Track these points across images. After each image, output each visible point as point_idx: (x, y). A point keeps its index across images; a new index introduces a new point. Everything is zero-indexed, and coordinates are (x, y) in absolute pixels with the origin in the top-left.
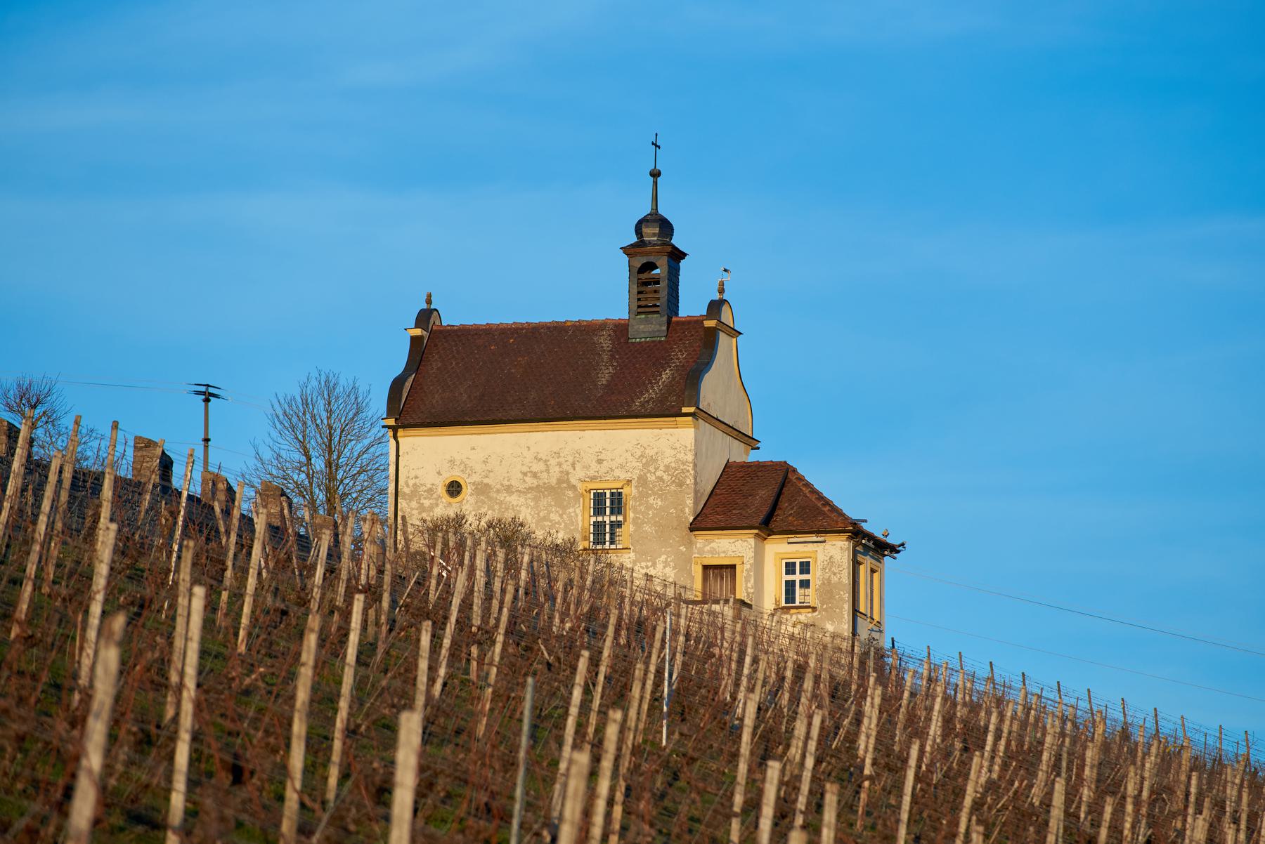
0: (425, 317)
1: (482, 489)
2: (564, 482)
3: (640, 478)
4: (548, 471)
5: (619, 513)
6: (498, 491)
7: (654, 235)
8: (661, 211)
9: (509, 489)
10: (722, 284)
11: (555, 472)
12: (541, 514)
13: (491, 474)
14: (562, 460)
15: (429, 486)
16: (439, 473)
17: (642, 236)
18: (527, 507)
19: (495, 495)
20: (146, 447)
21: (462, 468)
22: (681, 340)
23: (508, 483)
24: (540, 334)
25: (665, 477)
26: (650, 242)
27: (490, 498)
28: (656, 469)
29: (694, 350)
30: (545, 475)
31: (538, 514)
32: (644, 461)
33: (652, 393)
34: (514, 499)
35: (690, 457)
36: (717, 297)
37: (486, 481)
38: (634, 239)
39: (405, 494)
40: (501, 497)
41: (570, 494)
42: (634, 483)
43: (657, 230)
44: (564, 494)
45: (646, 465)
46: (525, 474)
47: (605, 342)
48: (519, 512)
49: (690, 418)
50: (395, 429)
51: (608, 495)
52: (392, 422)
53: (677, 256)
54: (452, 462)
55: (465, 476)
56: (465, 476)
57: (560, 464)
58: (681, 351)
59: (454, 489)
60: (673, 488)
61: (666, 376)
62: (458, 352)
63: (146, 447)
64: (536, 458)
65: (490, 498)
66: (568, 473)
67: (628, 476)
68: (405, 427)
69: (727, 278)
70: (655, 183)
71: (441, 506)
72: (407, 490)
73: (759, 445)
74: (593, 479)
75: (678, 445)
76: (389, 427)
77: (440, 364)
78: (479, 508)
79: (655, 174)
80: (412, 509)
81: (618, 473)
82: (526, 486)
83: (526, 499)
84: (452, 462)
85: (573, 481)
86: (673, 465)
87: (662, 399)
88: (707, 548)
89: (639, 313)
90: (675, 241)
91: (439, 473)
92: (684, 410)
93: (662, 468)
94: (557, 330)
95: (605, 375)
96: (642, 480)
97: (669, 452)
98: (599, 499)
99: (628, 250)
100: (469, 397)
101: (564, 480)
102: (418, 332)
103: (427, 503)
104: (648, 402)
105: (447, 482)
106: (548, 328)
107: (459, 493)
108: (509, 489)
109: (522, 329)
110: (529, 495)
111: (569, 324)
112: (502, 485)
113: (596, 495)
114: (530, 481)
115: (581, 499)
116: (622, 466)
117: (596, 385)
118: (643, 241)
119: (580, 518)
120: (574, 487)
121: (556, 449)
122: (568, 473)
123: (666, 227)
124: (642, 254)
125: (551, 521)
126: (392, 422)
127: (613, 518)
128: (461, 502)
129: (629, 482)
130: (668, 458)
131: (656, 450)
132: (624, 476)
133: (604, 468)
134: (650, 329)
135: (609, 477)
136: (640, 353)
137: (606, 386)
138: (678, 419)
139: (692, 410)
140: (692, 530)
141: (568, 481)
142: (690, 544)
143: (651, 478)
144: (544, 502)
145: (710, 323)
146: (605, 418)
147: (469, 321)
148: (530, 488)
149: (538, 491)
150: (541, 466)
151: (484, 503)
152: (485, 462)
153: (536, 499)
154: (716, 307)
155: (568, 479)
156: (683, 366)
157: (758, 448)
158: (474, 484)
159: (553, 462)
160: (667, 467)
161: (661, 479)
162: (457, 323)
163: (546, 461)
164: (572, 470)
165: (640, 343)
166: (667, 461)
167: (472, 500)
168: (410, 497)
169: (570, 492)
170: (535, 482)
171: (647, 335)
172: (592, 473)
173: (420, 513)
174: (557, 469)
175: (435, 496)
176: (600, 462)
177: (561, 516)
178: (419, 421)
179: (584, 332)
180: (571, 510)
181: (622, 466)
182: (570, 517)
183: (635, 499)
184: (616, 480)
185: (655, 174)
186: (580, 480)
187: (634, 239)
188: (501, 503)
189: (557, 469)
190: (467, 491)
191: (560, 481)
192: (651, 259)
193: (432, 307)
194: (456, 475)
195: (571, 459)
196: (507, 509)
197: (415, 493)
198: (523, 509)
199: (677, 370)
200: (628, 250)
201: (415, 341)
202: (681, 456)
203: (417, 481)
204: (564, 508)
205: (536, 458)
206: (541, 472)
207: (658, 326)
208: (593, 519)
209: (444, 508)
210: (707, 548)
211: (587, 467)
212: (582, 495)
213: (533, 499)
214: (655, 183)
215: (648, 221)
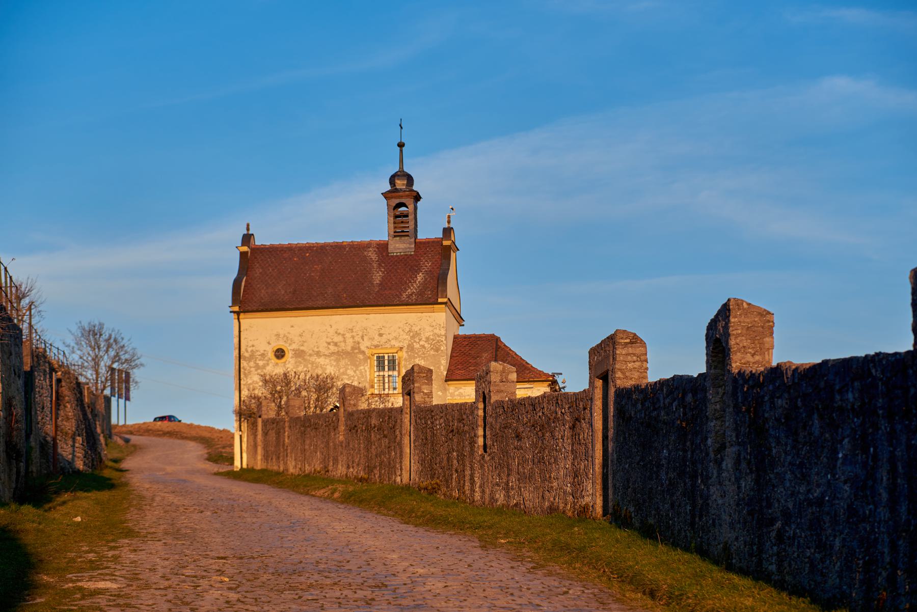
0: (247, 239)
1: (299, 354)
2: (356, 349)
3: (409, 346)
4: (345, 341)
5: (394, 369)
6: (310, 355)
8: (405, 170)
9: (318, 354)
10: (449, 217)
11: (350, 342)
12: (341, 371)
13: (305, 344)
14: (354, 334)
15: (262, 352)
16: (269, 343)
17: (395, 185)
18: (331, 366)
19: (308, 358)
20: (631, 343)
21: (285, 338)
22: (425, 254)
23: (317, 350)
24: (326, 250)
25: (426, 345)
26: (401, 189)
27: (304, 359)
28: (420, 340)
29: (435, 261)
30: (342, 344)
31: (339, 370)
32: (411, 334)
33: (413, 289)
34: (322, 361)
35: (443, 332)
36: (446, 225)
37: (302, 348)
40: (313, 359)
41: (361, 356)
42: (405, 350)
43: (405, 182)
44: (356, 357)
45: (412, 337)
46: (329, 344)
47: (372, 255)
48: (326, 369)
49: (444, 306)
50: (238, 313)
51: (386, 358)
52: (236, 309)
53: (417, 198)
54: (278, 335)
55: (287, 345)
56: (287, 345)
57: (353, 337)
58: (427, 261)
60: (432, 352)
61: (420, 277)
62: (272, 262)
63: (631, 343)
64: (336, 333)
65: (304, 359)
66: (359, 343)
67: (401, 345)
68: (245, 312)
69: (452, 214)
70: (401, 151)
71: (271, 365)
72: (247, 355)
73: (464, 323)
74: (376, 346)
75: (434, 324)
77: (261, 270)
78: (298, 366)
79: (401, 145)
80: (251, 367)
81: (393, 342)
82: (330, 351)
83: (330, 360)
85: (363, 348)
86: (431, 337)
87: (421, 293)
88: (457, 393)
89: (395, 236)
90: (415, 188)
91: (269, 343)
92: (440, 300)
93: (424, 339)
94: (338, 249)
95: (377, 277)
96: (411, 348)
97: (428, 328)
98: (380, 360)
99: (386, 195)
100: (286, 292)
101: (356, 347)
102: (245, 249)
103: (261, 363)
104: (411, 295)
105: (275, 349)
106: (332, 246)
107: (283, 356)
108: (318, 354)
109: (314, 247)
110: (332, 358)
111: (345, 244)
112: (313, 351)
113: (378, 357)
114: (333, 348)
115: (369, 361)
116: (396, 338)
117: (373, 284)
118: (396, 189)
119: (368, 373)
120: (363, 353)
121: (350, 327)
122: (359, 343)
123: (410, 179)
124: (396, 197)
125: (348, 375)
126: (236, 309)
127: (391, 373)
128: (285, 362)
129: (401, 348)
130: (428, 333)
131: (419, 327)
132: (397, 344)
134: (399, 247)
135: (388, 346)
136: (399, 263)
137: (380, 284)
138: (435, 306)
139: (445, 300)
140: (446, 381)
141: (359, 349)
142: (445, 390)
143: (417, 346)
144: (342, 363)
145: (446, 243)
146: (385, 306)
148: (333, 353)
149: (339, 355)
150: (340, 338)
151: (301, 363)
152: (301, 336)
153: (337, 361)
154: (448, 232)
155: (359, 347)
156: (430, 271)
157: (463, 325)
158: (293, 350)
159: (348, 335)
160: (428, 339)
161: (423, 347)
162: (268, 243)
163: (343, 335)
164: (362, 341)
165: (397, 256)
166: (427, 335)
167: (292, 361)
169: (361, 356)
171: (401, 251)
172: (375, 343)
173: (256, 370)
174: (351, 340)
175: (266, 358)
176: (381, 335)
177: (355, 372)
178: (255, 308)
179: (358, 249)
180: (362, 368)
181: (396, 338)
182: (361, 373)
183: (406, 360)
184: (392, 347)
185: (401, 145)
186: (367, 347)
188: (313, 363)
189: (351, 340)
190: (289, 355)
191: (353, 348)
192: (403, 200)
193: (250, 232)
194: (281, 344)
195: (360, 333)
196: (317, 367)
197: (252, 357)
199: (427, 274)
200: (386, 195)
201: (243, 255)
202: (437, 331)
203: (254, 348)
204: (357, 366)
205: (336, 333)
206: (340, 342)
207: (408, 245)
208: (377, 374)
209: (276, 369)
210: (457, 393)
211: (373, 339)
212: (369, 358)
213: (335, 361)
214: (401, 151)
215: (399, 176)
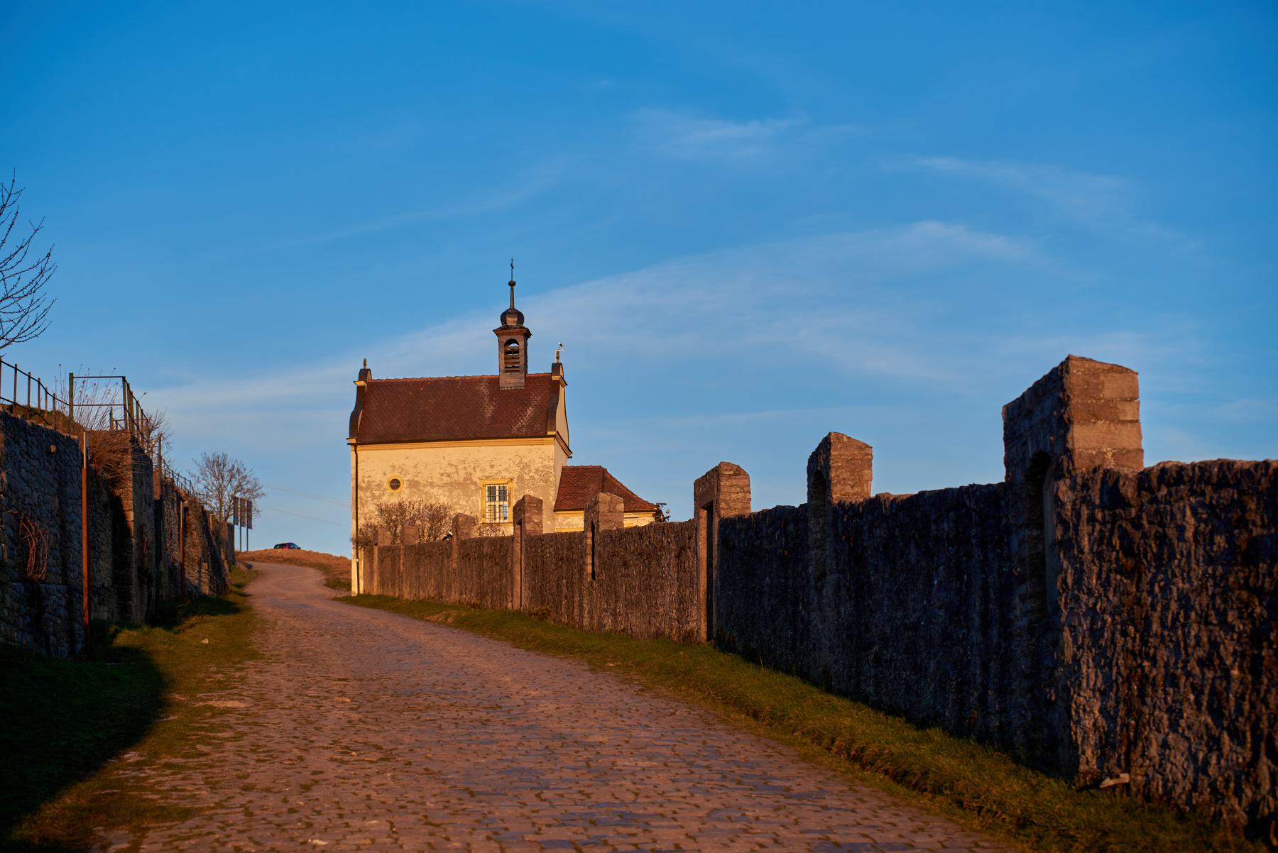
0: (364, 374)
1: (414, 485)
4: (457, 473)
5: (505, 500)
6: (424, 486)
7: (514, 322)
9: (432, 485)
10: (558, 353)
11: (462, 473)
12: (454, 501)
13: (419, 475)
14: (467, 465)
16: (385, 474)
20: (735, 475)
25: (536, 476)
27: (419, 490)
28: (530, 471)
30: (455, 475)
34: (435, 491)
35: (552, 464)
36: (555, 361)
37: (416, 479)
38: (499, 325)
39: (362, 488)
40: (427, 489)
41: (473, 487)
42: (515, 480)
46: (442, 475)
47: (484, 389)
48: (439, 499)
49: (552, 439)
50: (355, 445)
51: (497, 488)
52: (354, 441)
53: (527, 334)
55: (402, 476)
56: (402, 476)
57: (465, 468)
59: (395, 484)
60: (541, 483)
61: (530, 411)
63: (735, 475)
66: (471, 474)
67: (511, 476)
68: (361, 444)
70: (512, 290)
71: (386, 495)
72: (363, 485)
74: (488, 478)
75: (543, 456)
76: (351, 444)
79: (512, 284)
81: (504, 474)
84: (393, 467)
85: (474, 479)
87: (530, 427)
88: (565, 522)
89: (506, 372)
90: (525, 325)
91: (385, 474)
92: (549, 433)
95: (489, 411)
96: (520, 479)
97: (537, 460)
98: (491, 491)
99: (498, 332)
101: (468, 478)
102: (362, 383)
103: (377, 493)
105: (391, 480)
107: (398, 487)
108: (432, 485)
113: (489, 488)
116: (506, 470)
119: (480, 503)
120: (475, 483)
121: (462, 459)
122: (471, 474)
123: (520, 317)
126: (354, 441)
127: (501, 503)
129: (512, 480)
130: (537, 464)
132: (508, 476)
133: (495, 470)
134: (511, 382)
135: (499, 477)
137: (492, 417)
139: (554, 433)
140: (555, 511)
141: (471, 479)
142: (554, 519)
143: (526, 477)
144: (455, 493)
145: (555, 378)
147: (392, 377)
149: (452, 486)
150: (453, 470)
151: (415, 493)
152: (415, 467)
153: (450, 491)
154: (557, 367)
159: (461, 467)
160: (537, 470)
161: (533, 477)
162: (384, 378)
163: (456, 466)
166: (536, 466)
167: (407, 491)
168: (366, 489)
170: (449, 480)
172: (487, 474)
174: (464, 471)
176: (492, 466)
177: (467, 502)
178: (371, 440)
179: (468, 384)
181: (506, 470)
182: (473, 503)
183: (516, 490)
184: (503, 478)
185: (512, 284)
186: (479, 478)
187: (499, 325)
188: (427, 493)
189: (464, 471)
190: (404, 486)
191: (465, 479)
193: (367, 368)
194: (396, 475)
195: (472, 465)
196: (431, 497)
197: (368, 487)
198: (441, 497)
200: (498, 332)
201: (360, 389)
202: (546, 463)
204: (469, 497)
208: (488, 504)
209: (391, 499)
210: (565, 522)
211: (484, 470)
212: (481, 488)
214: (512, 290)
